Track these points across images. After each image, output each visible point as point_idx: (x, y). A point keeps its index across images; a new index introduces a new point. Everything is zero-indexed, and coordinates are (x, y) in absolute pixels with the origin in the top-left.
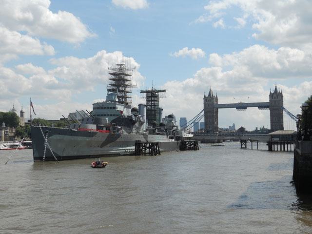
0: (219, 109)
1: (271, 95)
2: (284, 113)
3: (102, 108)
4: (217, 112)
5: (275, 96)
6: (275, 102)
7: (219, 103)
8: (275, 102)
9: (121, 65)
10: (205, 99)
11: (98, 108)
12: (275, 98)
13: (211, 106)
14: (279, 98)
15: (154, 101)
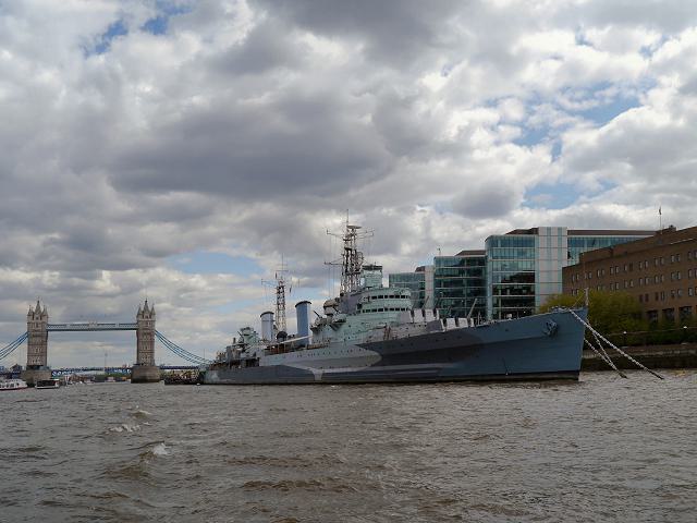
2: (156, 338)
3: (397, 297)
9: (353, 228)
11: (392, 297)
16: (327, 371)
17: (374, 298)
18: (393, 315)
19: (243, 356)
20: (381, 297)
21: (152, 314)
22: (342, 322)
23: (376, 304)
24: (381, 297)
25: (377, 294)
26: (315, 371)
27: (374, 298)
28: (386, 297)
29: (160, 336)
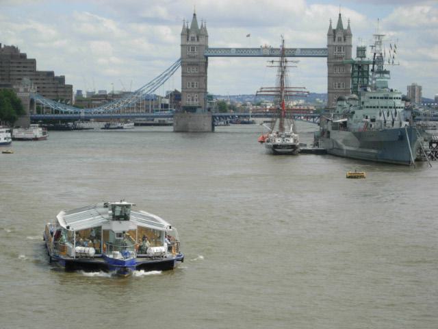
0: (209, 58)
1: (333, 34)
3: (386, 98)
4: (206, 63)
5: (339, 35)
7: (211, 45)
9: (379, 36)
10: (186, 33)
11: (382, 98)
12: (340, 39)
13: (195, 55)
14: (347, 43)
15: (363, 77)
16: (348, 148)
17: (371, 98)
20: (375, 98)
21: (347, 35)
24: (375, 98)
26: (345, 148)
27: (371, 98)
28: (378, 98)
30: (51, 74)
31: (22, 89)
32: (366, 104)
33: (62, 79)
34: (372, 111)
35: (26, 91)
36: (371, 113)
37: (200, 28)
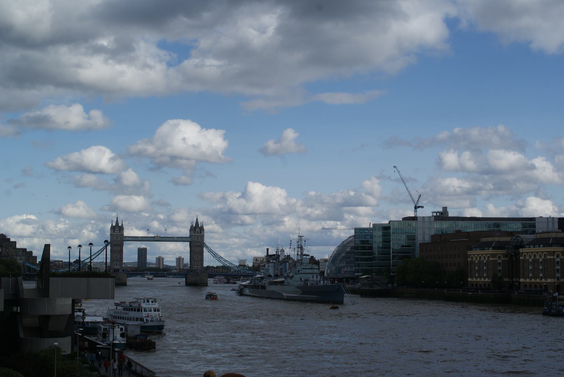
2: (205, 249)
5: (198, 230)
6: (198, 237)
8: (198, 237)
9: (301, 237)
10: (113, 228)
18: (308, 275)
19: (260, 284)
21: (202, 229)
22: (293, 276)
23: (304, 271)
25: (304, 267)
26: (285, 294)
29: (207, 247)
30: (26, 249)
31: (18, 258)
32: (300, 272)
33: (31, 253)
34: (305, 275)
35: (21, 259)
36: (304, 277)
37: (120, 225)
